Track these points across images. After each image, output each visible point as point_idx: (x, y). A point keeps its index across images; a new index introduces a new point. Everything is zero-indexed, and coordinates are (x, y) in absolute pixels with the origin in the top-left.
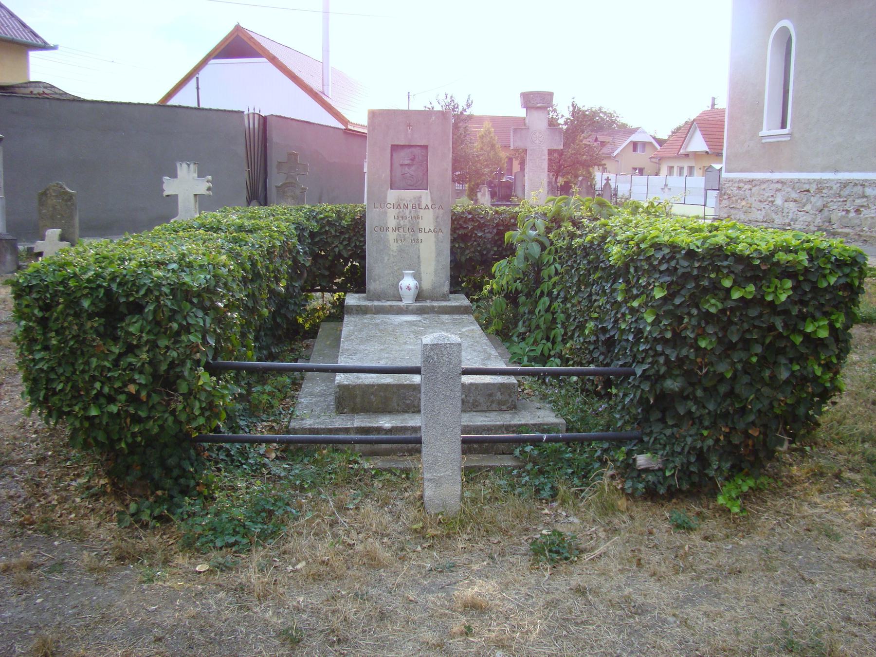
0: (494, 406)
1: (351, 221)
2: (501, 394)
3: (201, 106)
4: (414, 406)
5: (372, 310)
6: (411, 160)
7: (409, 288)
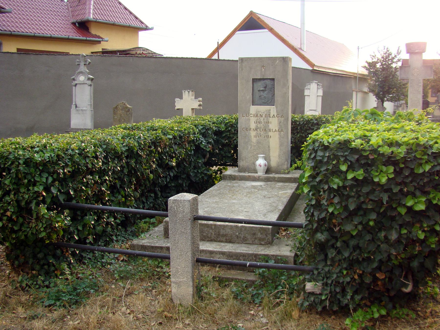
0: (256, 241)
2: (261, 234)
3: (220, 58)
4: (208, 237)
5: (238, 178)
7: (260, 166)
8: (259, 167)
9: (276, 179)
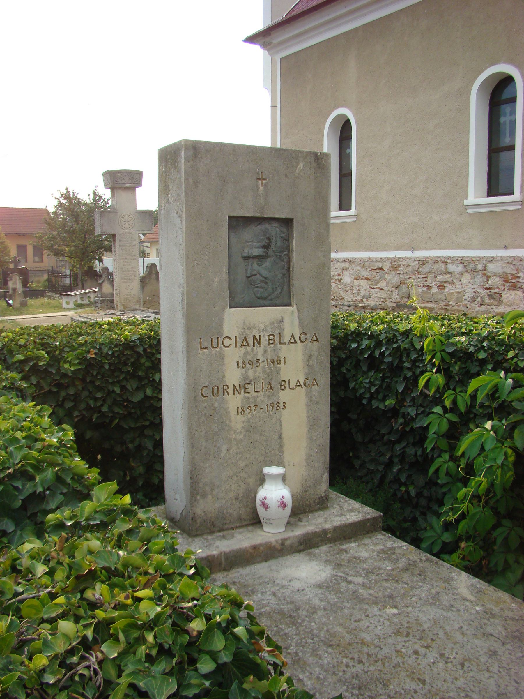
1: (79, 364)
5: (220, 564)
6: (264, 247)
8: (281, 509)
9: (329, 535)
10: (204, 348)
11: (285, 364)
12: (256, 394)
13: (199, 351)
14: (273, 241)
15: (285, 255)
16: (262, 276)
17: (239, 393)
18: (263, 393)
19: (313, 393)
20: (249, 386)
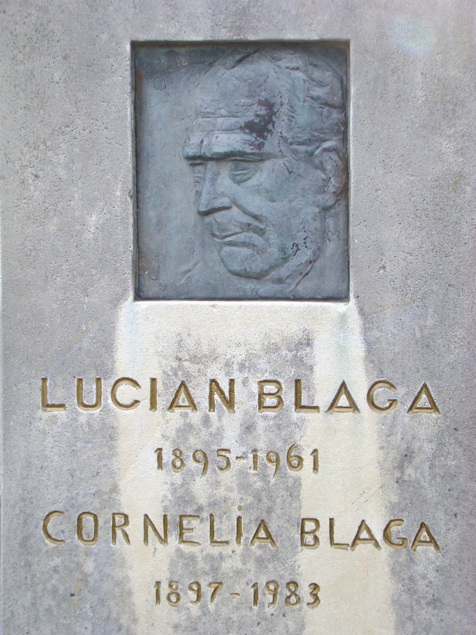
10: (53, 406)
11: (315, 468)
12: (216, 550)
13: (40, 413)
14: (285, 109)
15: (326, 150)
16: (245, 212)
17: (164, 541)
18: (239, 549)
19: (420, 569)
20: (195, 523)
